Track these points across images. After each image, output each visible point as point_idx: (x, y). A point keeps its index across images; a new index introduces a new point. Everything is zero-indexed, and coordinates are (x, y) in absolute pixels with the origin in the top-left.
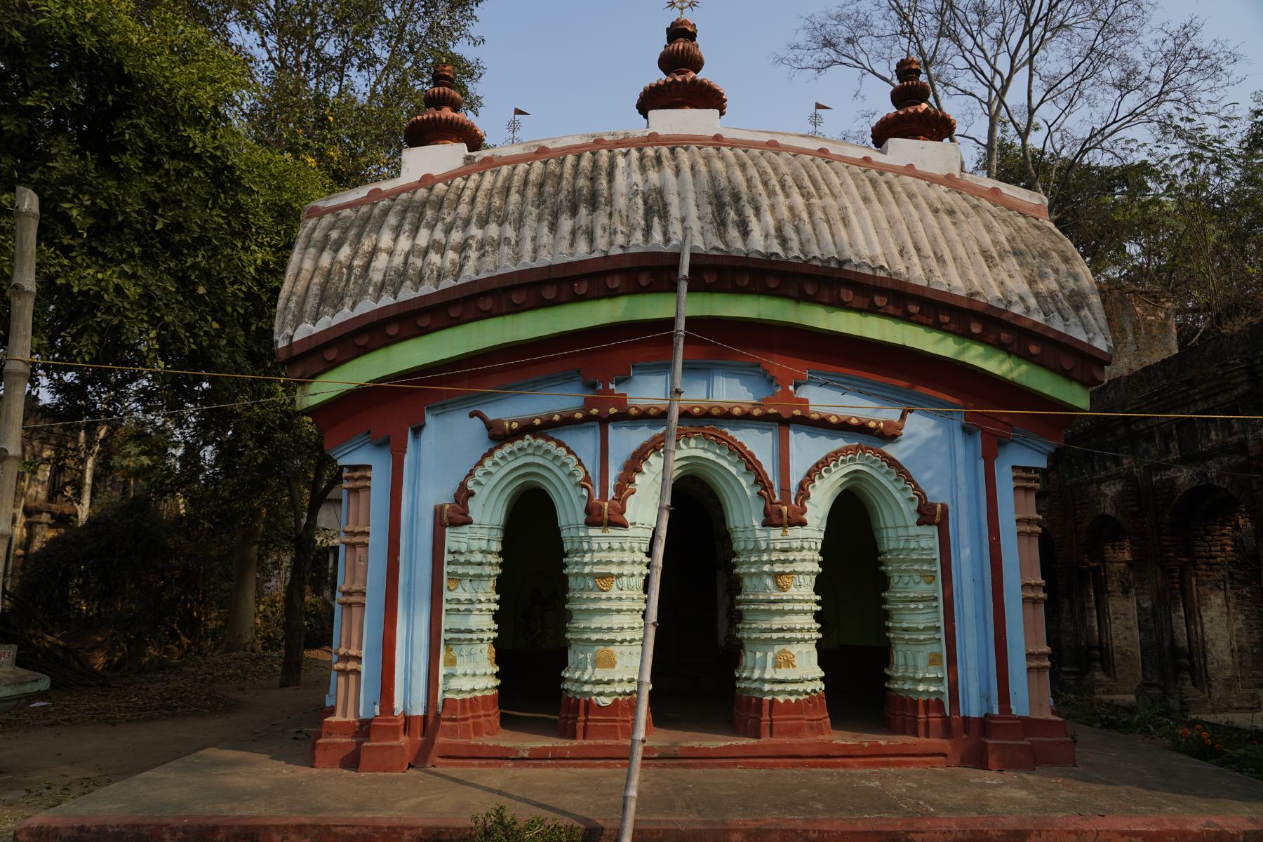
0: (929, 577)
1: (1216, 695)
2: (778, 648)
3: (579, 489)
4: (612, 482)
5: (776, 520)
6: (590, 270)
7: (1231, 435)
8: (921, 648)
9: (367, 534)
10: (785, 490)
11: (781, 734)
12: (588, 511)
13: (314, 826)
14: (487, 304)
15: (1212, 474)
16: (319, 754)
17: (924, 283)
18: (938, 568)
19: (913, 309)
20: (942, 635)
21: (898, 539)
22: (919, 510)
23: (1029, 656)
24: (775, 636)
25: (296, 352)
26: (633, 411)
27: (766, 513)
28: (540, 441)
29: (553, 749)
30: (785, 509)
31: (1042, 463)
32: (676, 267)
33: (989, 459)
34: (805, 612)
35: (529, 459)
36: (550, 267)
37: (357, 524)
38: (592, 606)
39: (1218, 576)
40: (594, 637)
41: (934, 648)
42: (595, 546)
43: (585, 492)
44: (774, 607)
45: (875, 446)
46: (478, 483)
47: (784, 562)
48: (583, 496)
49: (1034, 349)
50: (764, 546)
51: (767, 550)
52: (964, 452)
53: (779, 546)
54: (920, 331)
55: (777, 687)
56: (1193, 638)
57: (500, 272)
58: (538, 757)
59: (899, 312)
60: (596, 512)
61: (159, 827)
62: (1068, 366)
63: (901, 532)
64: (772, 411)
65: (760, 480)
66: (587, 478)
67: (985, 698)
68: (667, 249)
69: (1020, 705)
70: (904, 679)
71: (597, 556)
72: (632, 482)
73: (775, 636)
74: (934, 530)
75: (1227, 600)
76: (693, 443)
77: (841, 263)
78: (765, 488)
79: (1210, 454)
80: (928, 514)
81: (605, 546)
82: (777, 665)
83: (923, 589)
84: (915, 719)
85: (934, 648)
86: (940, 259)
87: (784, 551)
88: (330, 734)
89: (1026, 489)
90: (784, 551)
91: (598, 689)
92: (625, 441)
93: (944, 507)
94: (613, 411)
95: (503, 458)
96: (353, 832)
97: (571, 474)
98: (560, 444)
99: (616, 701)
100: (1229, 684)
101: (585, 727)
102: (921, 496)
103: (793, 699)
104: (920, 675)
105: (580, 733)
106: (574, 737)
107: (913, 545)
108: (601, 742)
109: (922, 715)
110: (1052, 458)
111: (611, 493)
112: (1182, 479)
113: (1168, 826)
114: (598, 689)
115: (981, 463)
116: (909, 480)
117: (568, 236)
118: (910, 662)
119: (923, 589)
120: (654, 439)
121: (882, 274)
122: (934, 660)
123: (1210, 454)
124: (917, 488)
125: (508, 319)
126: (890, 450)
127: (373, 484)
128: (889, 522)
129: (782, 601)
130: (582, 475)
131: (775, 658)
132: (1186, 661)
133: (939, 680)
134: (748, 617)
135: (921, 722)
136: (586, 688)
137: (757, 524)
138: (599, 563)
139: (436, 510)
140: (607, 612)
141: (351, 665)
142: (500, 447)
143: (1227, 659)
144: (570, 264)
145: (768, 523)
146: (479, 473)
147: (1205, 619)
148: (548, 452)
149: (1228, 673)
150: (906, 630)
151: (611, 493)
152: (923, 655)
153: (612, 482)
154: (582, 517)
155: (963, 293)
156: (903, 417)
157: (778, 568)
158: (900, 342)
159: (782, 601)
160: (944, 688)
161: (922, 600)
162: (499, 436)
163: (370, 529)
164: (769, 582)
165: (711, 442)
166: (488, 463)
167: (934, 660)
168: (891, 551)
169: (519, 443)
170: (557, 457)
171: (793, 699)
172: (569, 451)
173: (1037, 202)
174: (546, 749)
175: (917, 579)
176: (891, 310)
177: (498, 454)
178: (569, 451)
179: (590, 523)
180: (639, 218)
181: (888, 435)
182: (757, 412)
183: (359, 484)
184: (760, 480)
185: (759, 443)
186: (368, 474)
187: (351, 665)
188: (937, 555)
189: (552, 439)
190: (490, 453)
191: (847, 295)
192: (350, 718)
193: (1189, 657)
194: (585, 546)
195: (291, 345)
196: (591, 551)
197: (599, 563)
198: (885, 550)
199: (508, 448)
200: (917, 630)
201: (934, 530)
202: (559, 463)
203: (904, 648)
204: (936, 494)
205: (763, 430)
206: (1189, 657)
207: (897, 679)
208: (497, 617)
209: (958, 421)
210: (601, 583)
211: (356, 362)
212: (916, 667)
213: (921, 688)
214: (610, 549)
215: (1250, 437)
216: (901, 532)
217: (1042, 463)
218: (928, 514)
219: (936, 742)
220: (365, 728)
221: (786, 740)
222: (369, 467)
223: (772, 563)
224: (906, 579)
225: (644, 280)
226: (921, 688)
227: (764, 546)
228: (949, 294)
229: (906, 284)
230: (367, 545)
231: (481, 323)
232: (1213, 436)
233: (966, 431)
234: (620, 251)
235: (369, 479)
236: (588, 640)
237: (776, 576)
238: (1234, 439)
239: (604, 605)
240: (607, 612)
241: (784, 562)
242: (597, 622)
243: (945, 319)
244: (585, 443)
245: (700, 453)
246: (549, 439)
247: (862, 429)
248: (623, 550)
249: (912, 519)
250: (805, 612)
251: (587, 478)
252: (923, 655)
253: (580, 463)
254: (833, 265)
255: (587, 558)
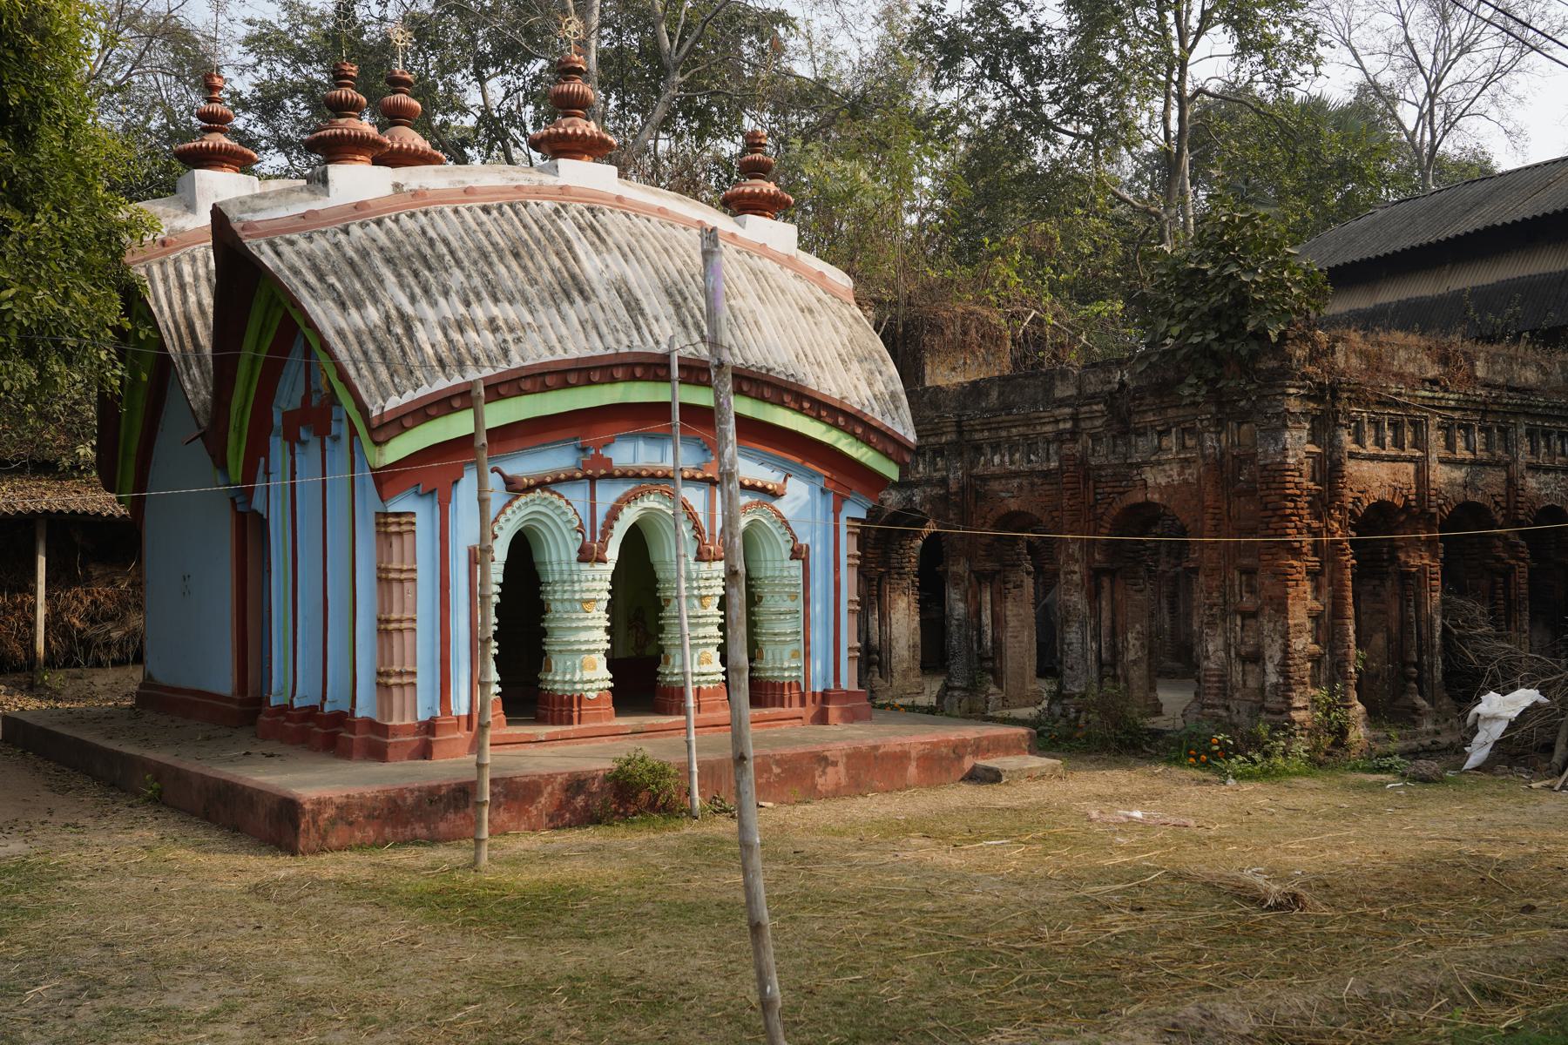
0: (794, 597)
1: (895, 684)
2: (701, 650)
3: (573, 534)
4: (599, 527)
5: (706, 556)
6: (605, 363)
7: (935, 471)
8: (786, 647)
9: (414, 570)
10: (712, 535)
11: (705, 711)
12: (581, 551)
13: (503, 779)
14: (527, 385)
15: (917, 499)
16: (390, 751)
17: (816, 388)
18: (801, 590)
19: (806, 405)
20: (801, 637)
21: (774, 569)
22: (792, 550)
23: (850, 649)
24: (701, 642)
25: (385, 421)
26: (617, 473)
27: (699, 552)
28: (547, 494)
29: (562, 732)
30: (712, 548)
31: (863, 516)
32: (668, 366)
33: (837, 511)
34: (712, 624)
35: (536, 508)
36: (578, 359)
37: (402, 562)
38: (581, 624)
39: (905, 585)
40: (584, 647)
41: (795, 646)
42: (583, 578)
43: (580, 536)
44: (701, 621)
45: (768, 501)
46: (501, 528)
47: (706, 587)
48: (577, 539)
49: (859, 430)
50: (695, 576)
51: (697, 579)
52: (822, 506)
53: (705, 576)
54: (806, 420)
55: (702, 678)
56: (883, 637)
57: (543, 360)
58: (551, 740)
59: (797, 407)
60: (588, 552)
61: (401, 790)
62: (890, 451)
63: (778, 564)
64: (709, 475)
65: (696, 527)
66: (581, 525)
67: (825, 679)
68: (659, 351)
69: (844, 685)
70: (773, 669)
71: (585, 586)
72: (612, 528)
73: (701, 642)
74: (799, 563)
75: (909, 605)
76: (652, 497)
77: (768, 370)
78: (700, 533)
79: (916, 484)
80: (798, 553)
81: (590, 578)
82: (700, 663)
83: (788, 605)
84: (782, 696)
85: (795, 646)
86: (819, 364)
87: (707, 579)
88: (395, 735)
89: (853, 533)
90: (707, 579)
91: (587, 686)
92: (608, 495)
93: (807, 546)
94: (603, 472)
95: (519, 508)
96: (527, 780)
97: (569, 521)
98: (561, 496)
99: (599, 695)
100: (905, 675)
101: (580, 716)
102: (794, 538)
103: (711, 686)
104: (786, 665)
105: (576, 719)
106: (570, 722)
107: (786, 574)
108: (592, 725)
109: (787, 692)
110: (869, 511)
111: (598, 537)
112: (890, 502)
113: (941, 738)
114: (587, 686)
115: (832, 516)
116: (789, 528)
117: (580, 328)
118: (778, 657)
119: (788, 605)
120: (626, 494)
121: (792, 380)
122: (795, 655)
123: (916, 484)
124: (792, 533)
125: (538, 396)
126: (776, 504)
127: (418, 528)
128: (769, 556)
129: (706, 616)
130: (577, 523)
131: (699, 657)
132: (876, 657)
133: (798, 668)
134: (557, 633)
135: (787, 697)
136: (578, 687)
137: (691, 559)
138: (588, 590)
139: (470, 551)
140: (577, 629)
141: (406, 680)
142: (517, 497)
143: (905, 653)
144: (592, 357)
145: (696, 560)
146: (502, 519)
147: (893, 621)
148: (552, 502)
149: (905, 665)
150: (775, 634)
151: (598, 537)
152: (787, 651)
153: (599, 527)
154: (575, 556)
155: (837, 397)
156: (785, 480)
157: (704, 592)
158: (794, 428)
159: (706, 616)
160: (801, 674)
161: (789, 613)
162: (514, 487)
163: (419, 566)
164: (696, 602)
165: (664, 497)
166: (509, 511)
167: (795, 655)
168: (766, 578)
169: (531, 496)
170: (559, 507)
171: (711, 686)
172: (568, 503)
173: (846, 284)
174: (557, 733)
175: (785, 598)
176: (792, 405)
177: (516, 504)
178: (568, 503)
179: (580, 560)
180: (627, 318)
181: (775, 495)
182: (699, 476)
183: (405, 528)
184: (696, 527)
185: (695, 497)
186: (413, 520)
187: (406, 680)
188: (801, 582)
189: (554, 492)
190: (510, 504)
191: (767, 393)
192: (408, 721)
193: (879, 653)
194: (576, 578)
195: (382, 414)
196: (580, 581)
197: (588, 590)
198: (762, 575)
199: (523, 499)
200: (785, 634)
201: (799, 563)
202: (559, 512)
203: (773, 647)
204: (804, 540)
205: (698, 488)
206: (879, 653)
207: (766, 670)
208: (608, 630)
209: (820, 483)
210: (586, 606)
211: (421, 428)
212: (782, 660)
213: (786, 674)
214: (594, 579)
215: (951, 476)
216: (778, 564)
217: (863, 516)
218: (798, 553)
219: (796, 709)
220: (430, 727)
221: (709, 715)
222: (413, 514)
223: (699, 588)
224: (777, 598)
225: (638, 372)
226: (786, 674)
227: (695, 576)
228: (830, 397)
229: (805, 388)
230: (414, 580)
231: (518, 399)
232: (921, 468)
233: (823, 491)
234: (627, 350)
235: (413, 524)
236: (579, 651)
237: (701, 598)
238: (937, 475)
239: (590, 623)
240: (577, 629)
241: (706, 587)
242: (583, 636)
243: (824, 413)
244: (578, 496)
245: (656, 505)
246: (553, 493)
247: (764, 490)
248: (594, 579)
249: (787, 554)
250: (712, 624)
251: (581, 525)
252: (787, 651)
253: (576, 513)
254: (764, 371)
255: (577, 587)
